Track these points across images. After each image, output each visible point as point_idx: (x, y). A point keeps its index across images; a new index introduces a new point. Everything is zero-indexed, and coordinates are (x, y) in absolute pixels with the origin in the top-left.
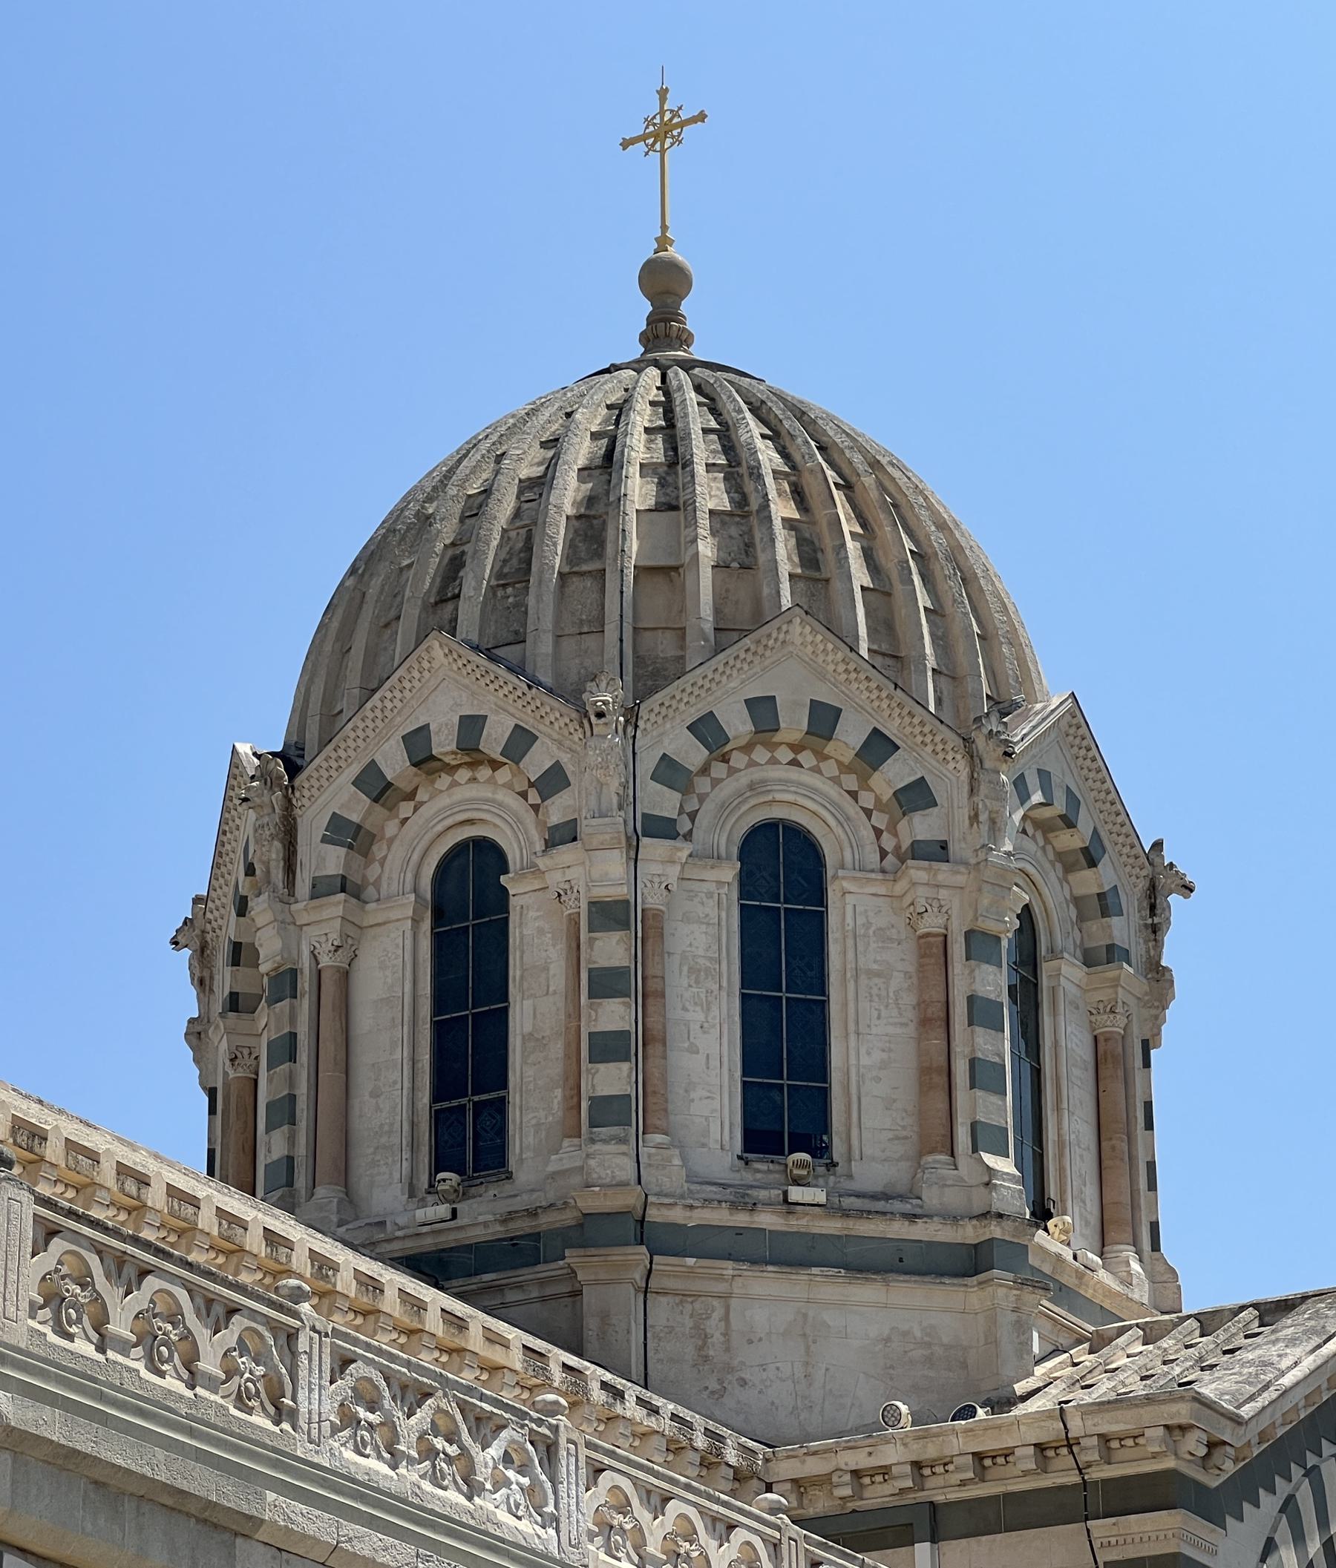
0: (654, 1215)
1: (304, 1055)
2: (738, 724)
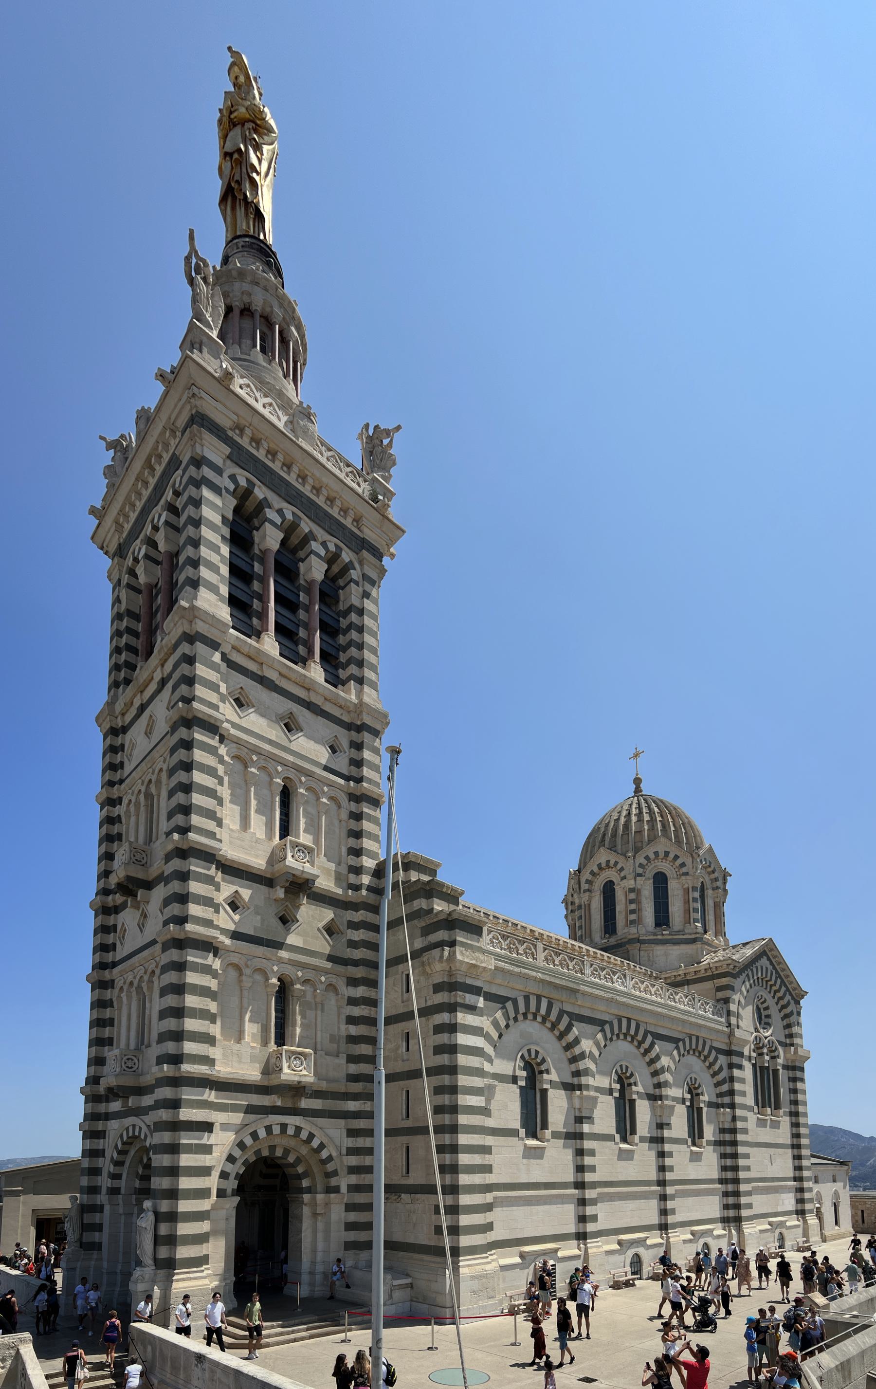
0: (641, 938)
1: (583, 918)
2: (652, 856)
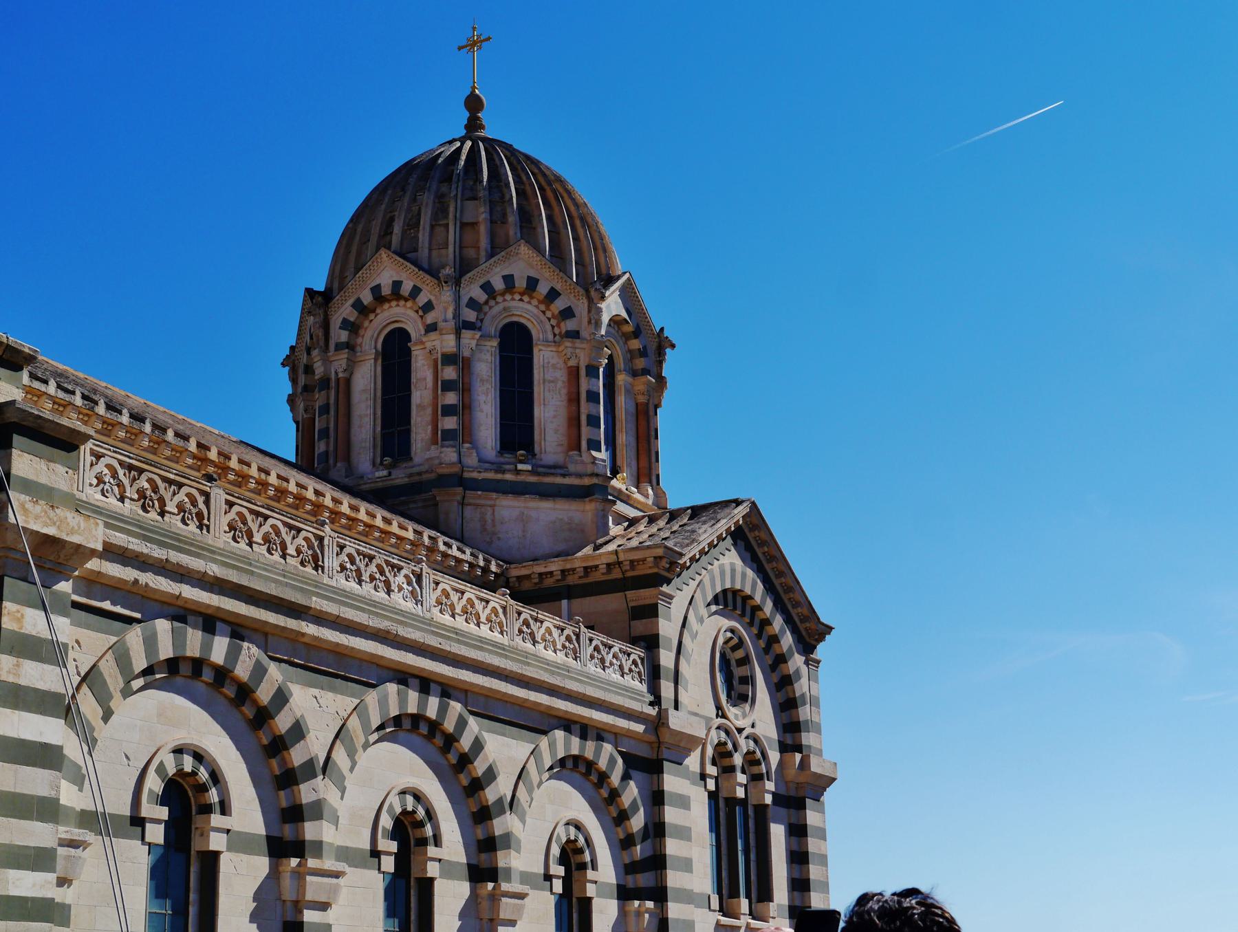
0: (466, 475)
1: (332, 412)
2: (499, 285)
